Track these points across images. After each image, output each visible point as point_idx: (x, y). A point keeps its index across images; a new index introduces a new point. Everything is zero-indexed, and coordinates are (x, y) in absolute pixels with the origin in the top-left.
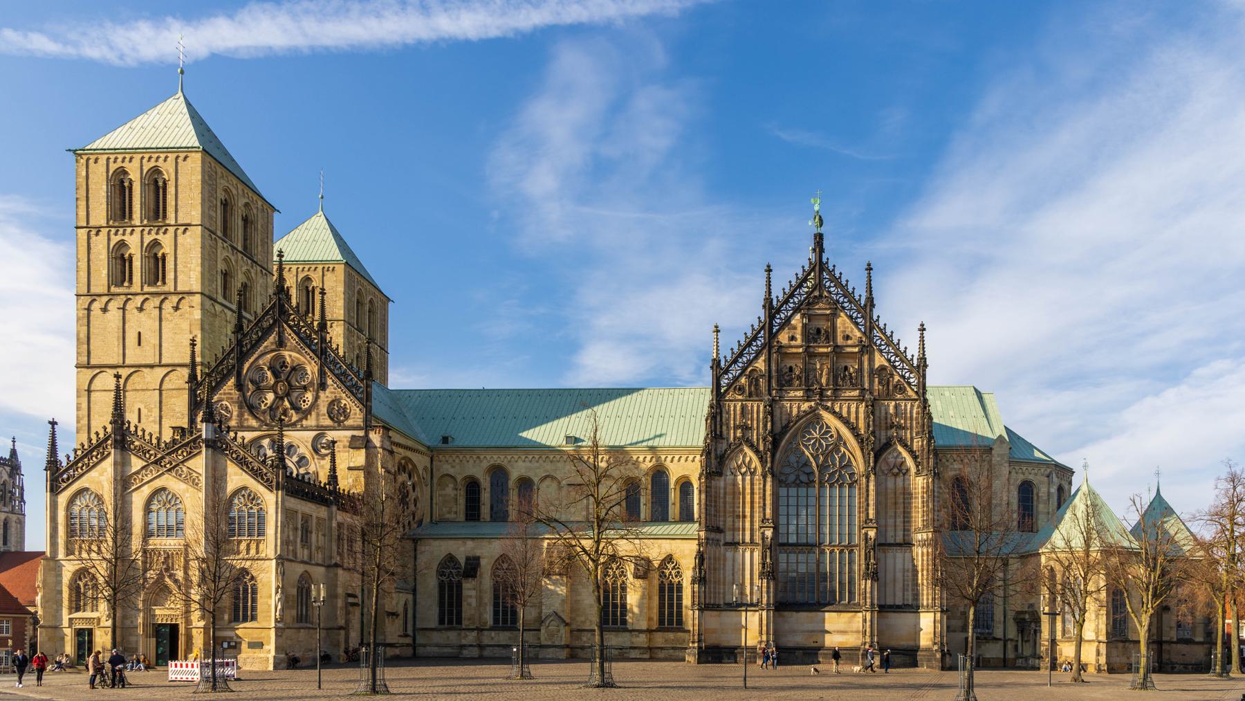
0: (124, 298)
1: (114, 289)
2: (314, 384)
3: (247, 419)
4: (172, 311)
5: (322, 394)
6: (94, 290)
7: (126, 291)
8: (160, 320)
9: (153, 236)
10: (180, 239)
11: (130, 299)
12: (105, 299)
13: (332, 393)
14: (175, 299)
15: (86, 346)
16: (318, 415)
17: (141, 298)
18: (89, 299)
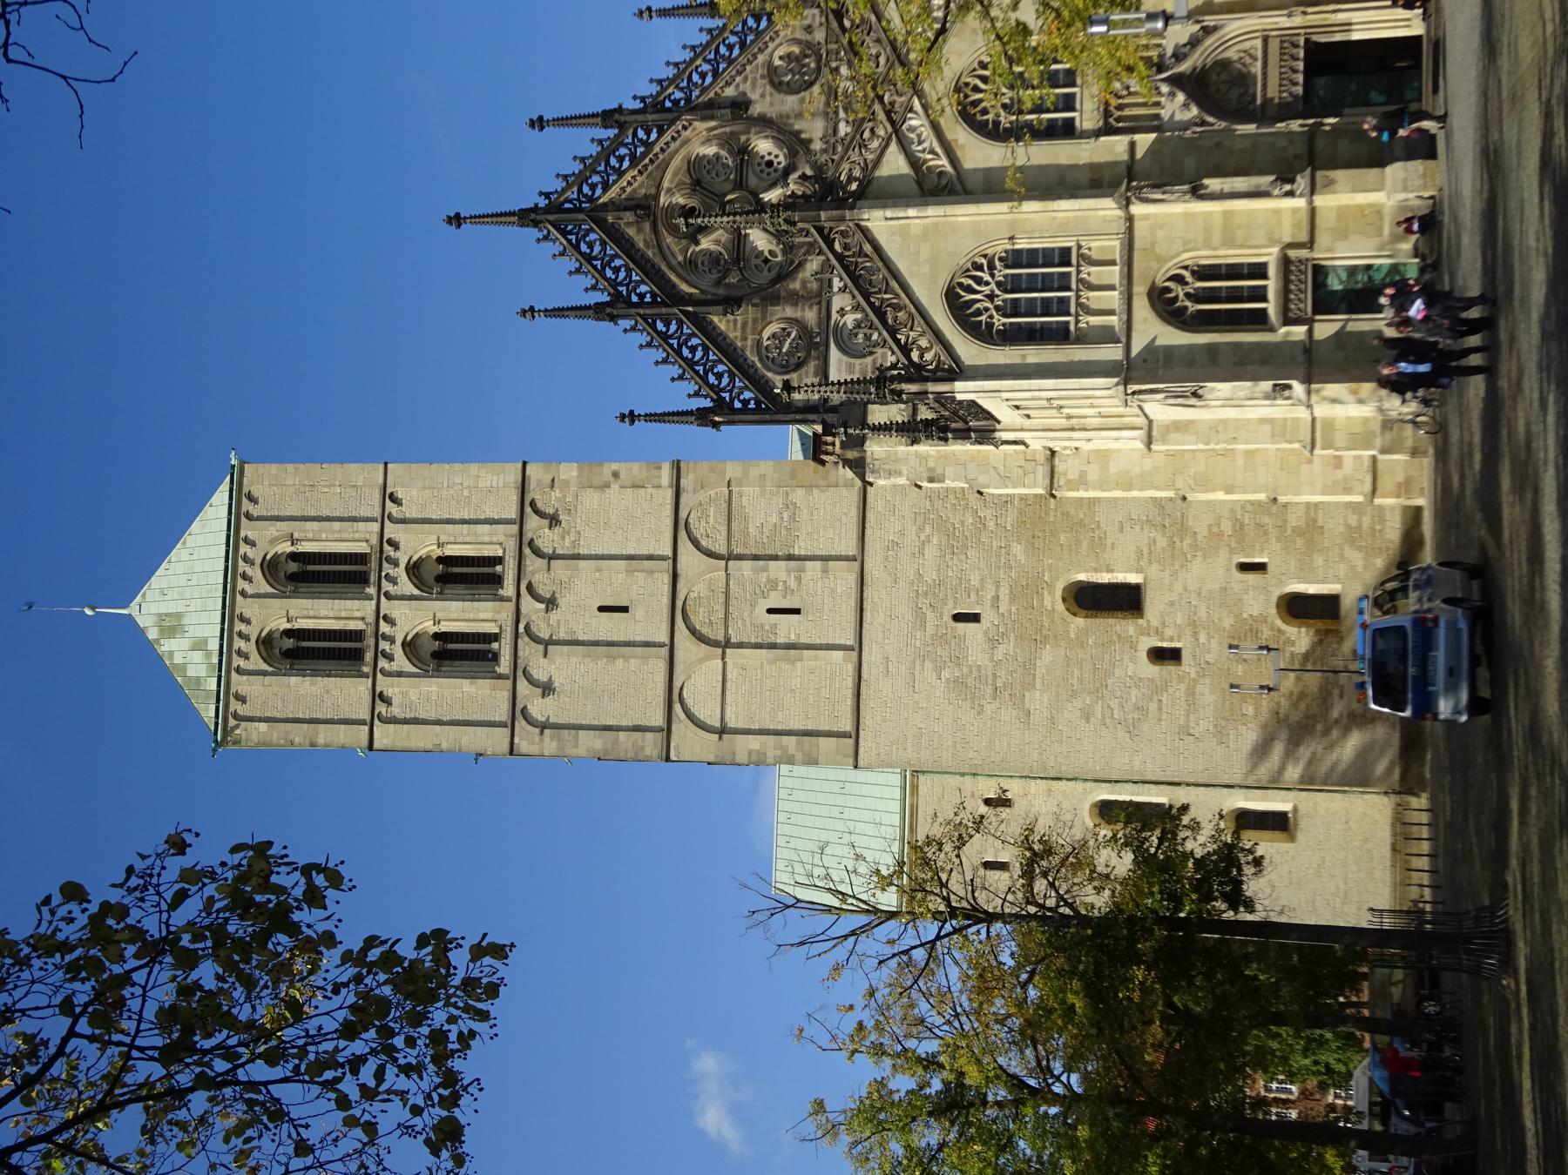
0: (524, 641)
1: (504, 666)
2: (732, 133)
3: (804, 282)
4: (557, 530)
5: (756, 110)
6: (502, 714)
7: (507, 639)
8: (577, 557)
9: (400, 574)
10: (410, 511)
11: (527, 628)
12: (523, 686)
13: (754, 86)
14: (533, 522)
15: (622, 734)
16: (800, 115)
17: (527, 600)
18: (521, 723)
